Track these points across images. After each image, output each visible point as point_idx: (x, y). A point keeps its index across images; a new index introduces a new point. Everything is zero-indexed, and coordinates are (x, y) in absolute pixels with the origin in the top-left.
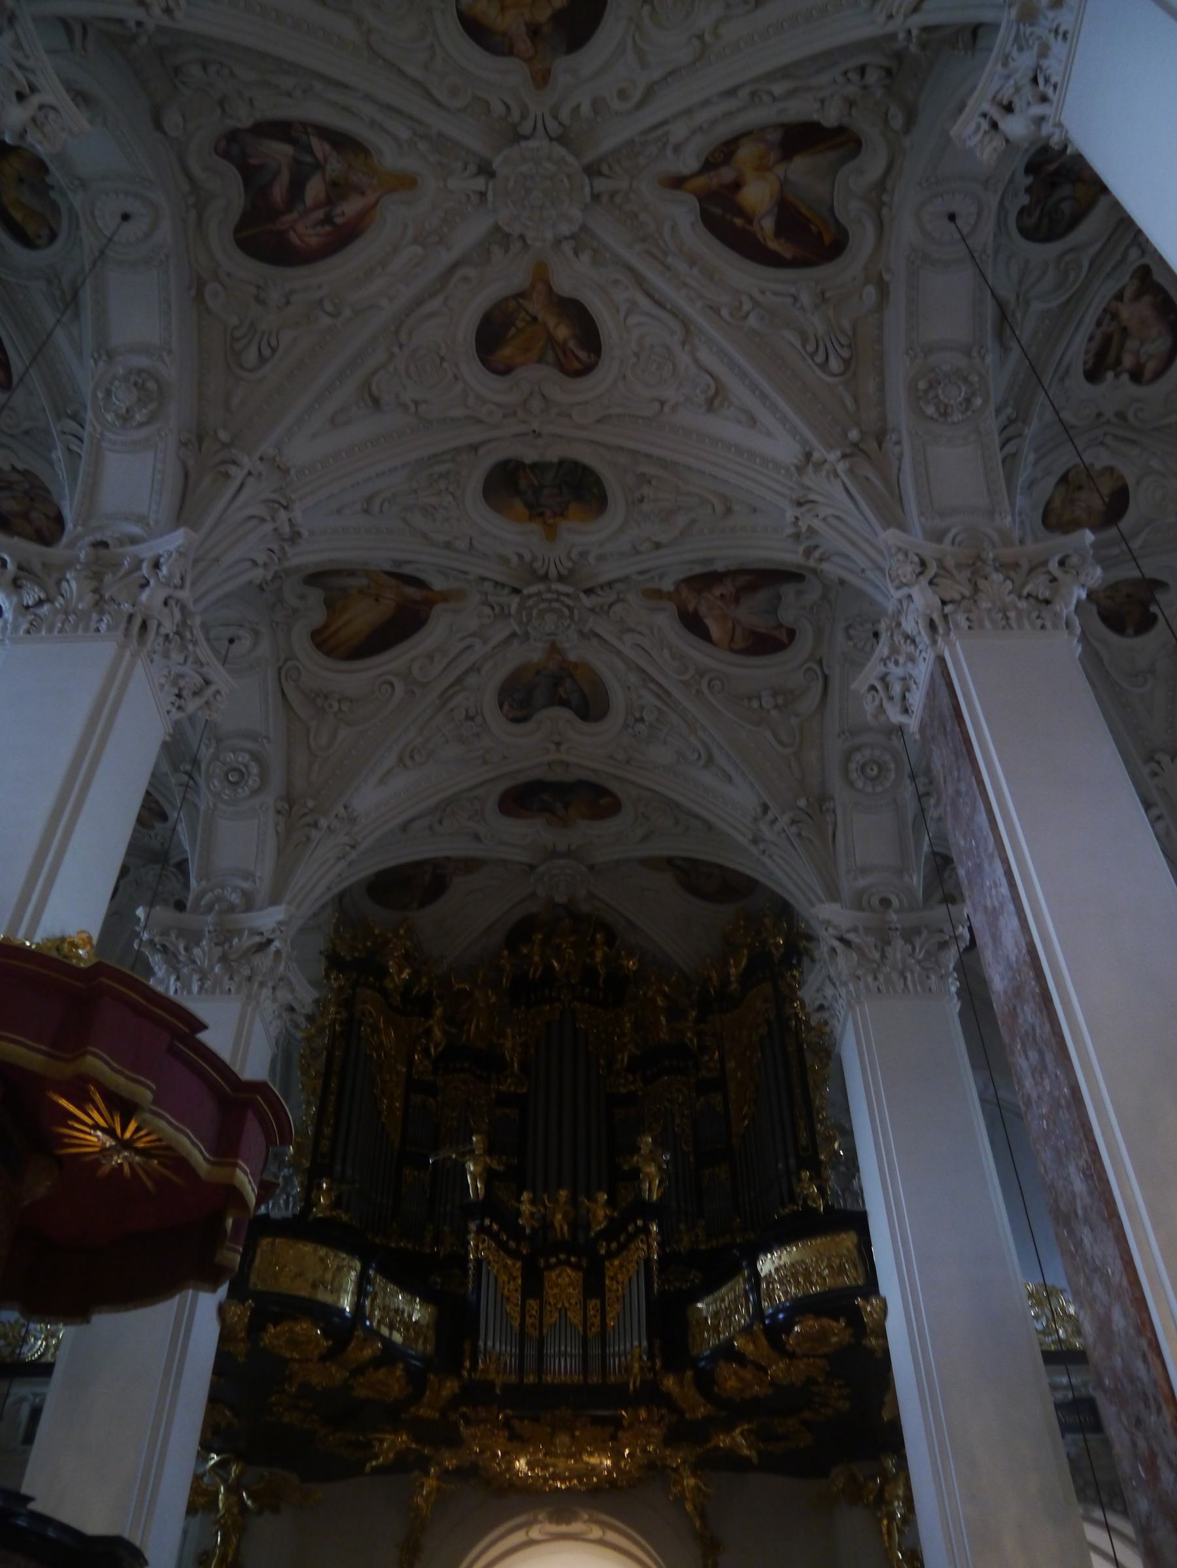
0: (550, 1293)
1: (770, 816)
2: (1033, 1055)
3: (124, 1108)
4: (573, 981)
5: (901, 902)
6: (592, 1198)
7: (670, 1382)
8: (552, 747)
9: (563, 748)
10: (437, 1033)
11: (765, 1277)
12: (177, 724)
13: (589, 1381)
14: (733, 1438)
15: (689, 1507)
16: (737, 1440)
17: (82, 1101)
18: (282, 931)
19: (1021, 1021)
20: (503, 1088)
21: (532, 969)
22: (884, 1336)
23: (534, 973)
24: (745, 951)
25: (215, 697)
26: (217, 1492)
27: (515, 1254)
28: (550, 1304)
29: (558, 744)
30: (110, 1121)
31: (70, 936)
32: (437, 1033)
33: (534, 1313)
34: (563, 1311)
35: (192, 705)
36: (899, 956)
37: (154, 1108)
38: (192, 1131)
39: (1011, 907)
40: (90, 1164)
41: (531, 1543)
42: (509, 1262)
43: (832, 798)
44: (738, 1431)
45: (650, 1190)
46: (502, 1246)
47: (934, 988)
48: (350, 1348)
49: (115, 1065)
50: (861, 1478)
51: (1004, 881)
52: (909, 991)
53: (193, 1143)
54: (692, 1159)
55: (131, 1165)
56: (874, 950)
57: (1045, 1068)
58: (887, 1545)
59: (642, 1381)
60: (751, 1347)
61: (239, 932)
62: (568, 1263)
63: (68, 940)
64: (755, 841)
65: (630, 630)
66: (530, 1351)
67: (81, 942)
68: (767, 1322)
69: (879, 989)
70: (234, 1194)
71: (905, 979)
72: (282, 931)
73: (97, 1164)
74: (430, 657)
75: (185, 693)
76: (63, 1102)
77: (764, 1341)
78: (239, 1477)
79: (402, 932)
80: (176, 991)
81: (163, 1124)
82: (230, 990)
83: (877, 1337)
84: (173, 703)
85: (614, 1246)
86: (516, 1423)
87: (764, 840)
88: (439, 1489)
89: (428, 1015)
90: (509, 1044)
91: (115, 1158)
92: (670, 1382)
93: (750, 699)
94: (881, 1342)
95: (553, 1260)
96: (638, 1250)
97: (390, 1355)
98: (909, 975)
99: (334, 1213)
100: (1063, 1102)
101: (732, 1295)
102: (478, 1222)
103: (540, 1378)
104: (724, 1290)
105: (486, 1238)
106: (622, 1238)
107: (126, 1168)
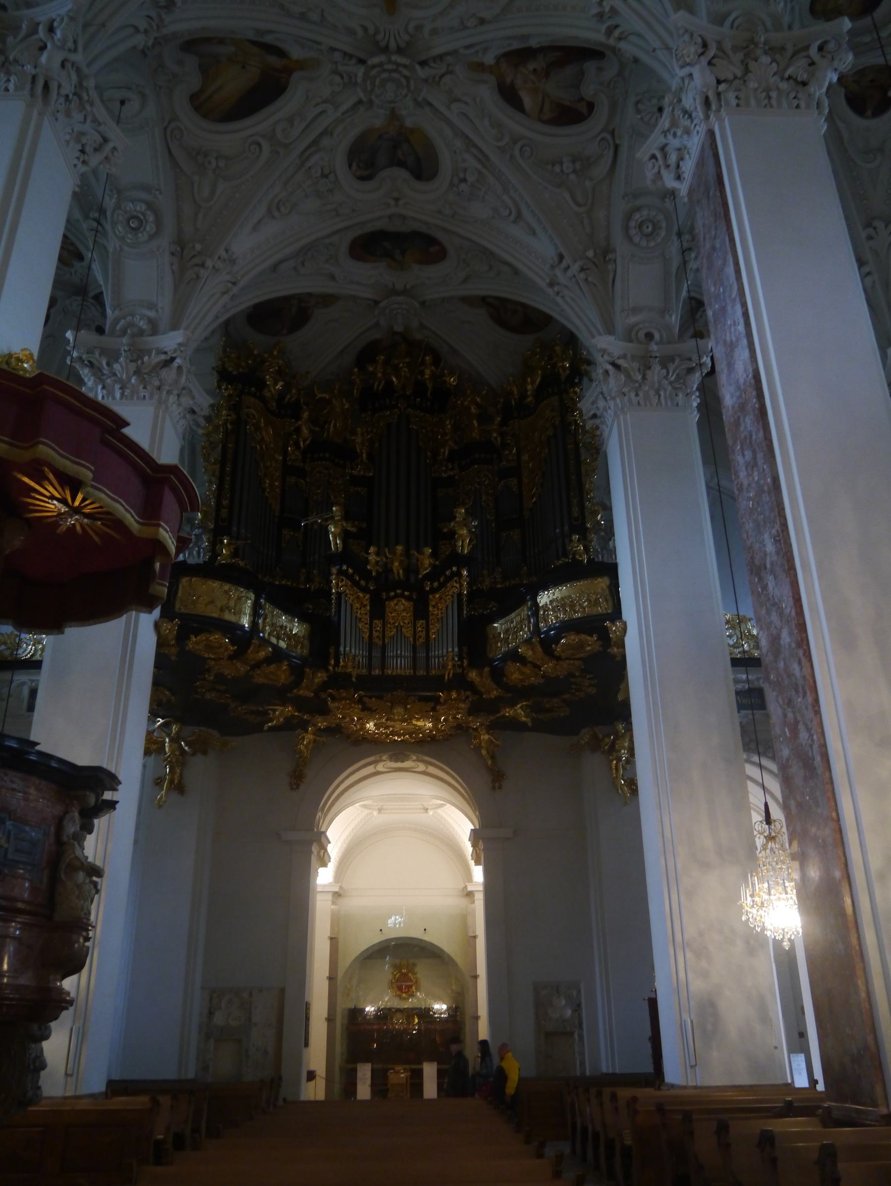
0: (390, 616)
1: (564, 264)
2: (748, 454)
3: (73, 484)
4: (408, 393)
5: (661, 337)
6: (420, 551)
7: (473, 675)
8: (392, 202)
9: (401, 202)
10: (305, 431)
11: (543, 606)
12: (83, 176)
14: (515, 710)
15: (484, 752)
16: (518, 712)
17: (40, 478)
18: (181, 351)
19: (742, 428)
20: (355, 472)
21: (376, 384)
22: (623, 646)
23: (379, 386)
24: (540, 372)
25: (113, 153)
26: (164, 742)
27: (365, 590)
28: (390, 623)
29: (397, 200)
30: (63, 493)
31: (16, 354)
32: (305, 431)
33: (378, 629)
34: (399, 629)
35: (95, 160)
36: (656, 378)
37: (93, 483)
38: (124, 501)
39: (745, 342)
40: (51, 525)
41: (377, 773)
42: (361, 595)
43: (614, 251)
44: (518, 706)
45: (462, 546)
46: (356, 584)
47: (680, 403)
48: (249, 651)
49: (61, 452)
50: (601, 736)
51: (742, 321)
52: (661, 405)
53: (126, 509)
54: (493, 525)
55: (81, 525)
56: (637, 374)
57: (755, 464)
58: (615, 775)
59: (454, 674)
60: (530, 653)
61: (149, 352)
62: (402, 596)
63: (14, 356)
64: (551, 285)
65: (456, 100)
66: (377, 654)
67: (24, 358)
68: (542, 636)
69: (639, 403)
70: (159, 547)
71: (659, 396)
72: (181, 351)
73: (56, 525)
74: (290, 120)
75: (88, 149)
76: (26, 480)
77: (539, 649)
78: (177, 733)
79: (275, 353)
80: (103, 397)
81: (103, 496)
82: (144, 396)
83: (618, 648)
84: (78, 158)
85: (436, 584)
86: (366, 700)
87: (558, 284)
88: (315, 741)
89: (298, 418)
90: (359, 440)
91: (69, 520)
92: (473, 675)
93: (553, 165)
94: (620, 650)
95: (392, 594)
96: (453, 587)
97: (278, 655)
98: (662, 393)
99: (233, 561)
100: (766, 488)
101: (518, 618)
103: (383, 672)
104: (513, 615)
105: (344, 578)
106: (442, 579)
107: (78, 528)
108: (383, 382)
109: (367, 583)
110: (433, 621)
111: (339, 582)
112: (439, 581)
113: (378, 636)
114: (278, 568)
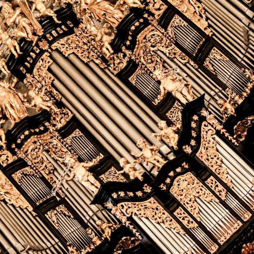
4: (41, 34)
13: (245, 220)
20: (59, 126)
23: (16, 50)
27: (146, 197)
28: (187, 203)
33: (184, 215)
34: (197, 199)
45: (184, 96)
46: (135, 199)
54: (192, 63)
66: (201, 235)
85: (193, 143)
95: (168, 181)
96: (208, 134)
102: (110, 199)
106: (194, 134)
108: (16, 44)
109: (142, 190)
110: (217, 171)
111: (122, 210)
112: (193, 138)
113: (189, 221)
114: (69, 247)
